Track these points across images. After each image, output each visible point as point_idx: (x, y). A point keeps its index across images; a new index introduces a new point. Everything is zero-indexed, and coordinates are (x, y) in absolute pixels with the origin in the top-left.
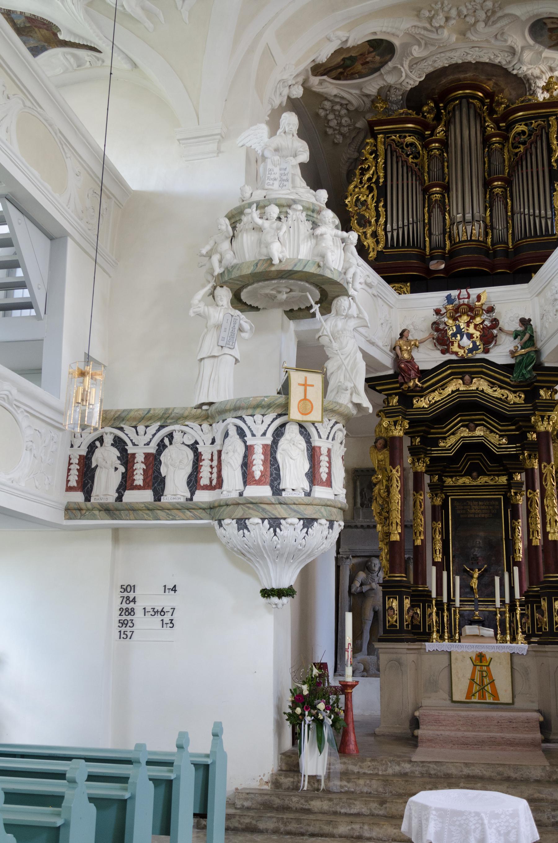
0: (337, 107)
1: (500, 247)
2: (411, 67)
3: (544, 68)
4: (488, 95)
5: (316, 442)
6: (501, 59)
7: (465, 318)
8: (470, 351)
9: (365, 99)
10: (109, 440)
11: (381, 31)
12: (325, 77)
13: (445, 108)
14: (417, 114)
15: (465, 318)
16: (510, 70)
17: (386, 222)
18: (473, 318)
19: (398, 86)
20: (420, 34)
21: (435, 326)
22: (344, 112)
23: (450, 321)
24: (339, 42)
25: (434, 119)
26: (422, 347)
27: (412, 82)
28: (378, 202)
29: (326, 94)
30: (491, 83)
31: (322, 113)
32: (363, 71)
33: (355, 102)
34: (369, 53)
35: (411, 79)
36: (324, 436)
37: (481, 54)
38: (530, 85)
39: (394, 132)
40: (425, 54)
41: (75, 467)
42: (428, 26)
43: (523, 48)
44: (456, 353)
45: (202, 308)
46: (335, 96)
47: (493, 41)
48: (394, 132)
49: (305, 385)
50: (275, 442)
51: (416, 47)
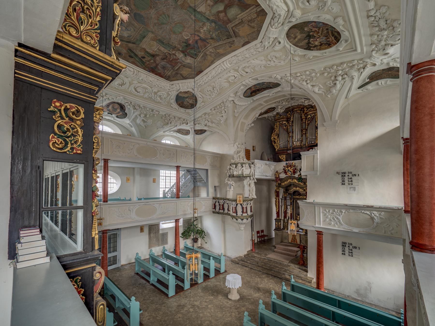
1: (304, 146)
4: (302, 108)
5: (243, 206)
7: (290, 168)
8: (291, 174)
10: (217, 201)
15: (290, 168)
17: (279, 143)
18: (291, 168)
21: (284, 169)
23: (287, 169)
26: (282, 174)
28: (278, 138)
36: (245, 205)
39: (281, 121)
41: (213, 205)
44: (288, 175)
45: (227, 181)
48: (281, 121)
49: (240, 197)
50: (236, 206)
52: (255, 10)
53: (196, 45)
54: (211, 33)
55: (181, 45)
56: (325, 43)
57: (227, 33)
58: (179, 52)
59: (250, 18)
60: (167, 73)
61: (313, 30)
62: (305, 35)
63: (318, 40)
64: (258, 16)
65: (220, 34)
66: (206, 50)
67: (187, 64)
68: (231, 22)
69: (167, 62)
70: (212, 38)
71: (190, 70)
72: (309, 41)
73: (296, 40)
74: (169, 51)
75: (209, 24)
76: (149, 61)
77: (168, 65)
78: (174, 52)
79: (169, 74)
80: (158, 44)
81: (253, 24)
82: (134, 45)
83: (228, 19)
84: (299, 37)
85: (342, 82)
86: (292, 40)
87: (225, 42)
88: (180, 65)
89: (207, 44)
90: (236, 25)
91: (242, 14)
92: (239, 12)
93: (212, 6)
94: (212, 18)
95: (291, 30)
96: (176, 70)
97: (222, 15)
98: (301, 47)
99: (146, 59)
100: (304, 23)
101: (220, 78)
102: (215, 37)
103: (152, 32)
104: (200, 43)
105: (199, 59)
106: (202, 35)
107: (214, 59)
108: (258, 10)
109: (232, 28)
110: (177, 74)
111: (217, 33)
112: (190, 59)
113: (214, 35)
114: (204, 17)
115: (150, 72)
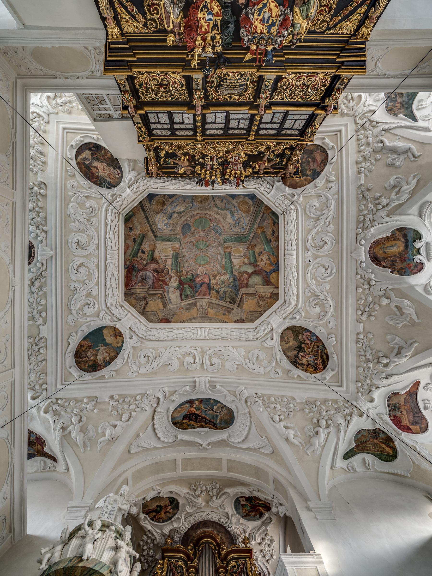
0: (149, 541)
2: (185, 519)
3: (242, 531)
4: (218, 545)
6: (223, 520)
9: (163, 537)
11: (176, 493)
12: (147, 516)
13: (198, 550)
14: (185, 549)
16: (227, 528)
19: (178, 530)
20: (190, 498)
22: (152, 545)
24: (157, 492)
25: (193, 555)
27: (184, 528)
29: (146, 528)
30: (219, 537)
31: (142, 543)
32: (165, 518)
33: (158, 538)
34: (169, 506)
35: (185, 526)
37: (215, 515)
38: (236, 540)
40: (191, 511)
42: (193, 494)
43: (232, 515)
46: (149, 531)
47: (219, 508)
51: (188, 506)
52: (272, 290)
53: (198, 286)
54: (223, 286)
55: (187, 275)
56: (312, 364)
57: (235, 296)
58: (178, 279)
59: (263, 295)
60: (137, 287)
61: (306, 342)
62: (297, 344)
63: (306, 357)
64: (271, 297)
65: (228, 292)
66: (200, 300)
67: (167, 298)
68: (247, 288)
69: (154, 276)
70: (218, 292)
71: (161, 307)
72: (298, 353)
73: (288, 345)
74: (172, 270)
75: (229, 277)
76: (142, 259)
77: (150, 282)
78: (173, 275)
79: (138, 290)
80: (172, 256)
81: (261, 303)
82: (153, 237)
83: (247, 284)
84: (291, 344)
85: (326, 431)
86: (284, 343)
87: (224, 304)
88: (161, 292)
89: (207, 294)
90: (248, 294)
91: (261, 286)
92: (260, 283)
93: (246, 264)
94: (236, 273)
95: (287, 331)
96: (148, 294)
97: (246, 276)
98: (288, 357)
99: (143, 256)
100: (302, 328)
101: (179, 347)
102: (221, 293)
103: (181, 244)
104: (204, 288)
105: (183, 304)
106: (213, 282)
107: (196, 318)
108: (275, 292)
109: (243, 294)
110: (144, 298)
111: (227, 289)
112: (177, 296)
113: (222, 290)
114: (232, 268)
115: (125, 268)
